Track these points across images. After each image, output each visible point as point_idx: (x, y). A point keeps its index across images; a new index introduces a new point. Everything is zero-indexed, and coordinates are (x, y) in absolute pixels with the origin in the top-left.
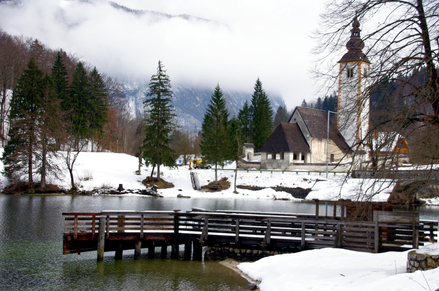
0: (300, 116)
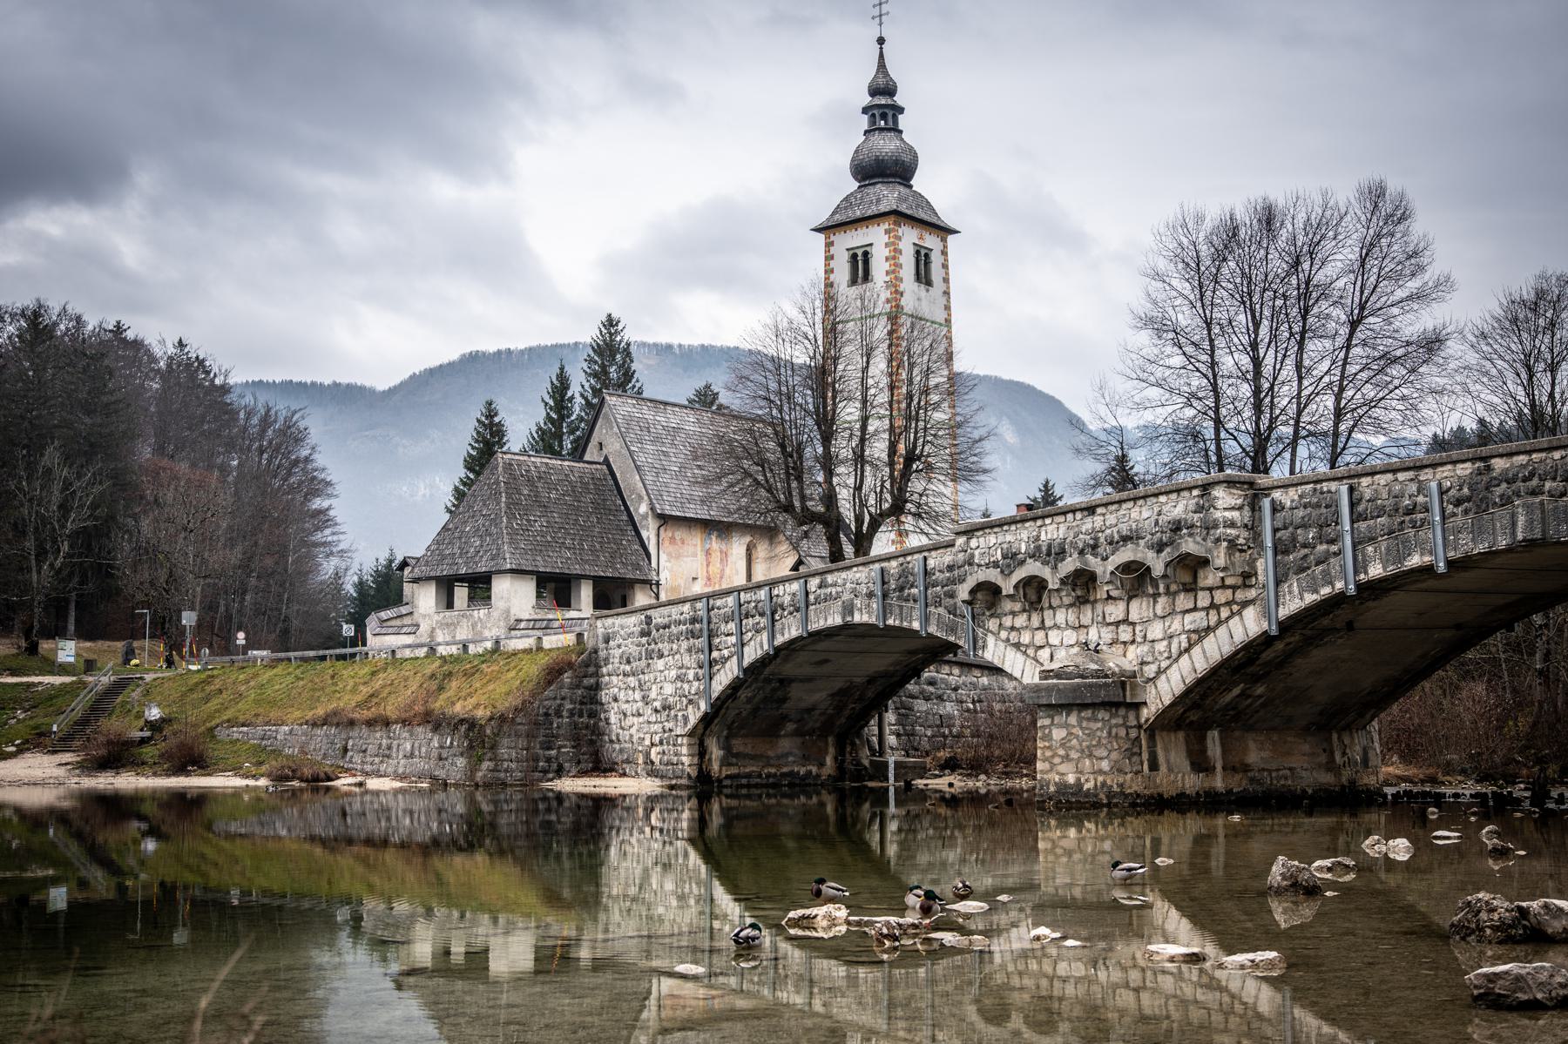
0: (616, 429)
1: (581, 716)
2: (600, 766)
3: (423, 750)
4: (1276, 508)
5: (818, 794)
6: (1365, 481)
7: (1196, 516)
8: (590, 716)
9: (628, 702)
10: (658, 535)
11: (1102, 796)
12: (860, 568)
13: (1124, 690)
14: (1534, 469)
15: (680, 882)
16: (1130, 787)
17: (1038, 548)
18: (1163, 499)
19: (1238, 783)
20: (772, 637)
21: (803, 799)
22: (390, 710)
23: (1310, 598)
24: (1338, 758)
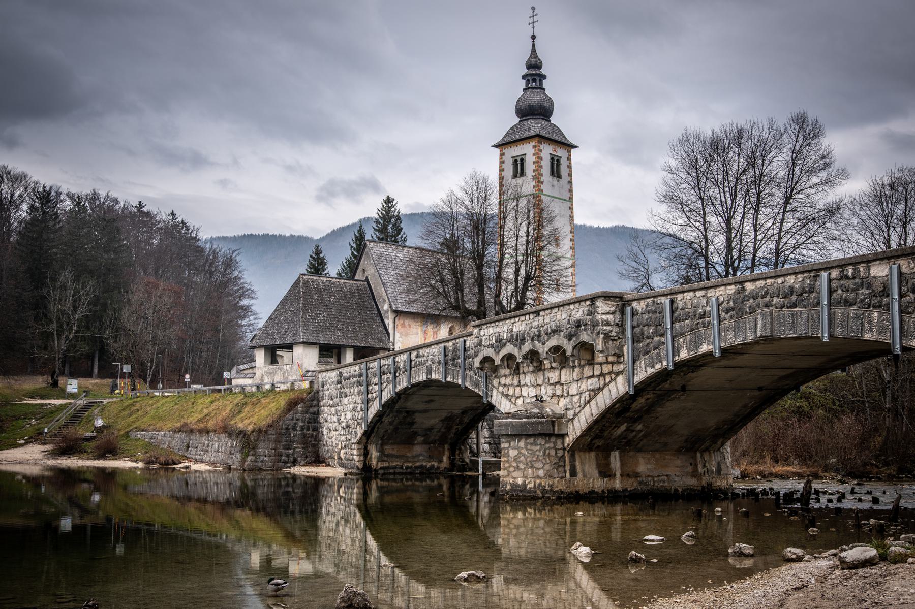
0: (372, 261)
1: (308, 430)
2: (318, 460)
3: (223, 448)
4: (634, 313)
5: (438, 479)
6: (680, 297)
7: (588, 317)
8: (313, 430)
9: (331, 422)
10: (394, 323)
11: (539, 492)
12: (435, 346)
13: (553, 426)
14: (768, 290)
15: (352, 530)
16: (557, 487)
17: (512, 336)
18: (572, 307)
19: (631, 485)
20: (395, 387)
21: (428, 482)
22: (211, 424)
23: (650, 371)
24: (700, 469)
